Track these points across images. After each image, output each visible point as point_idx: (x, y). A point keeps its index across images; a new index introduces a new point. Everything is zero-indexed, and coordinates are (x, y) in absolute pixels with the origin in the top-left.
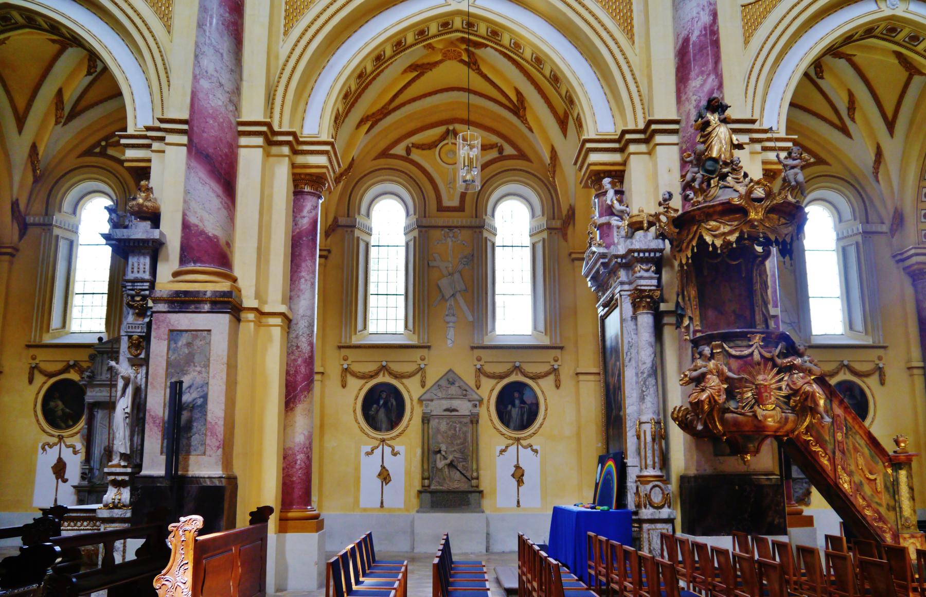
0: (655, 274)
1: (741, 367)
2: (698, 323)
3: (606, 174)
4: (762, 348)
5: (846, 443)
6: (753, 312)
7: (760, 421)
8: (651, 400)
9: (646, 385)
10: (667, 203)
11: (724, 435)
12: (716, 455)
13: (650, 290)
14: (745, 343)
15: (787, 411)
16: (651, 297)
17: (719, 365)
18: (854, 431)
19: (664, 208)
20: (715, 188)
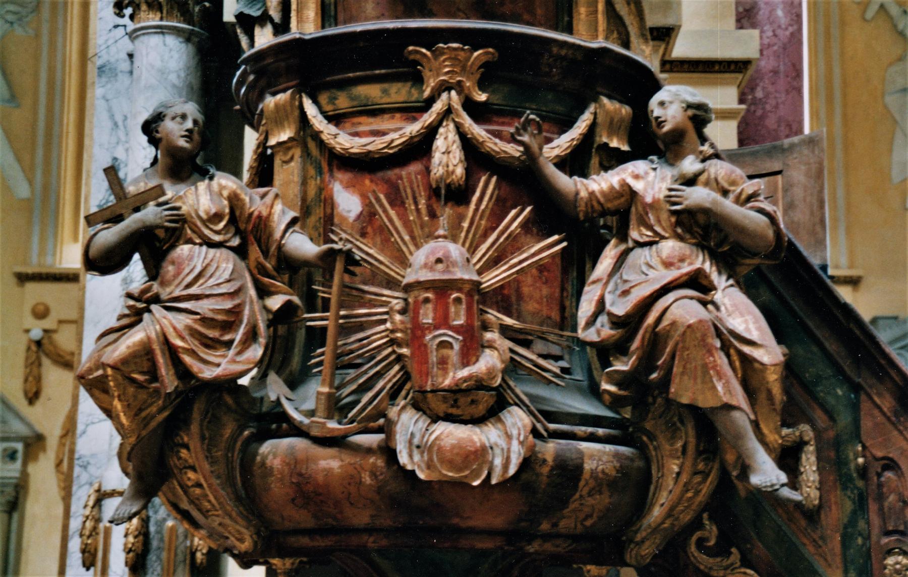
14: (399, 93)
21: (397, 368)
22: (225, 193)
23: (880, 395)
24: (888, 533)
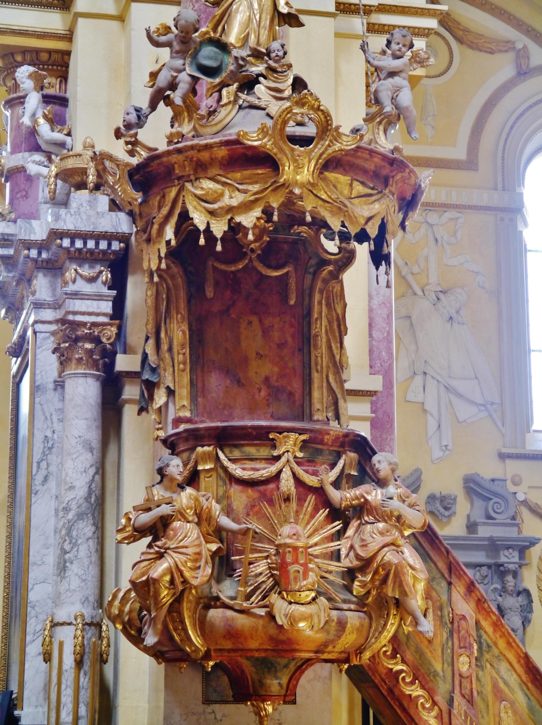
0: (109, 288)
1: (253, 506)
2: (185, 403)
3: (28, 57)
4: (298, 464)
5: (478, 679)
6: (308, 382)
7: (281, 627)
8: (81, 572)
9: (71, 537)
10: (132, 132)
11: (207, 656)
12: (207, 701)
14: (264, 452)
15: (345, 606)
16: (97, 340)
17: (202, 500)
18: (496, 651)
19: (127, 143)
20: (230, 107)
21: (271, 579)
22: (192, 497)
23: (459, 586)
24: (461, 648)
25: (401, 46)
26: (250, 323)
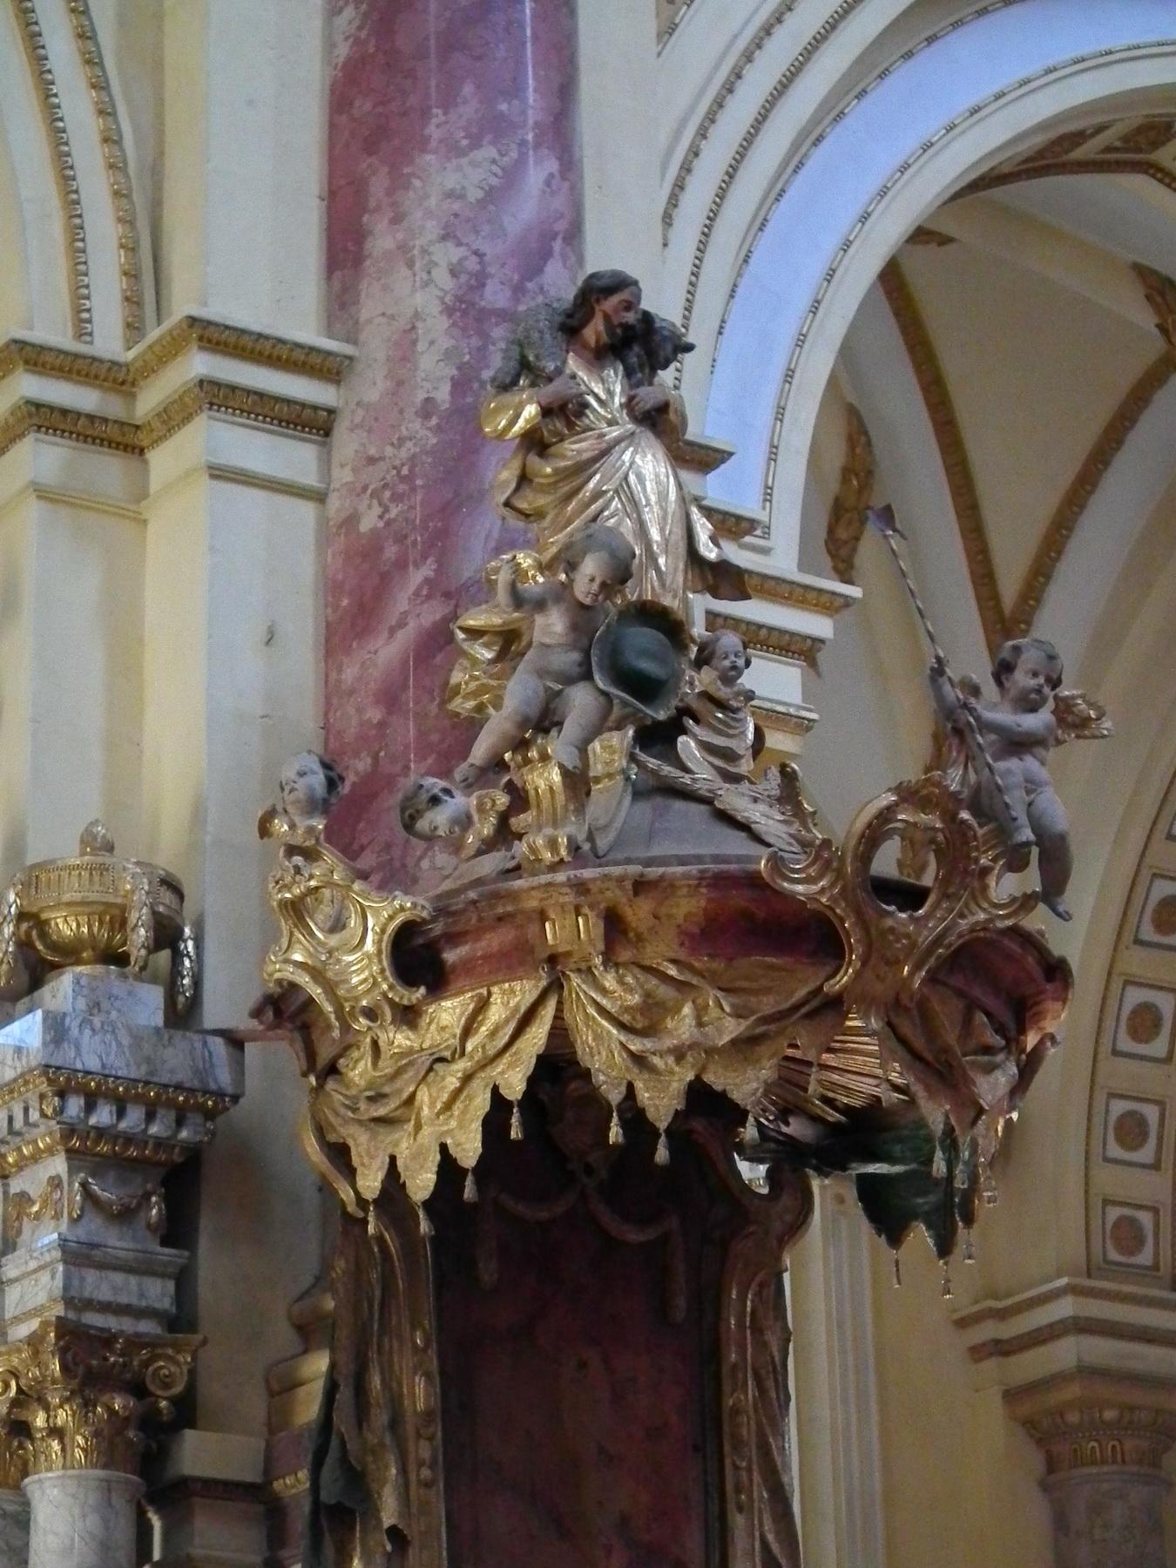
0: (165, 1242)
13: (136, 1342)
25: (1041, 680)
26: (583, 1365)
